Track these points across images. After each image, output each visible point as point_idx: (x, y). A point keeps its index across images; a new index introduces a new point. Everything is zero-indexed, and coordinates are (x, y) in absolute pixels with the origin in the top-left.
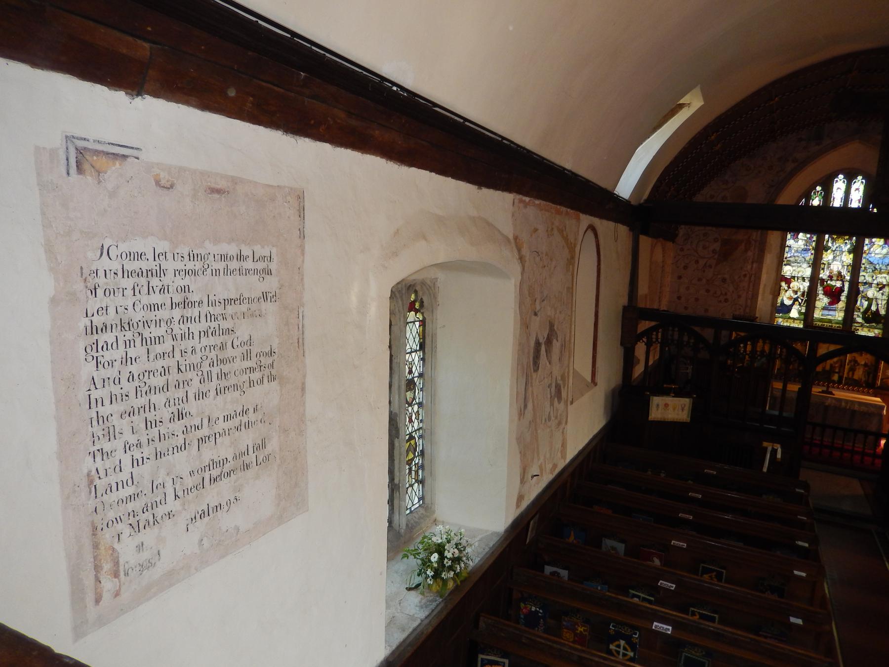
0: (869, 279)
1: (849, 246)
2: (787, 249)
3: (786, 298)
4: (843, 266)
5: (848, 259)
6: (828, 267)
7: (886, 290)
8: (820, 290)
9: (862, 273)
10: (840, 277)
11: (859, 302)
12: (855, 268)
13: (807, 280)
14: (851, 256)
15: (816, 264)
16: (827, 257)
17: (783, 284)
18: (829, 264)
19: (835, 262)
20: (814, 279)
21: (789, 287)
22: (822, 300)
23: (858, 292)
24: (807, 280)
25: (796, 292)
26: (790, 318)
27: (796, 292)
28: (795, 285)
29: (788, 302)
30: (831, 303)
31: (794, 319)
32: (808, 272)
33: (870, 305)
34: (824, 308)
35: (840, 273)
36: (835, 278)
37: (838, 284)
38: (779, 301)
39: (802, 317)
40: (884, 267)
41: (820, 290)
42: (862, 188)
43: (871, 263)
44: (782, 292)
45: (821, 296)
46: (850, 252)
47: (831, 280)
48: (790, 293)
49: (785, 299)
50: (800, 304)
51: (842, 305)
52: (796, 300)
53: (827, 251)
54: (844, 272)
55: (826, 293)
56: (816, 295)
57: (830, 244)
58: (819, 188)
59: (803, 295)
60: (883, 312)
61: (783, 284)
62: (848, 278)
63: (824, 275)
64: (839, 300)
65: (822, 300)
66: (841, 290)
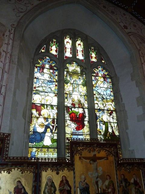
0: (102, 107)
1: (82, 81)
2: (35, 80)
3: (38, 125)
4: (81, 96)
5: (83, 90)
6: (70, 97)
7: (114, 114)
8: (67, 117)
9: (96, 102)
10: (81, 105)
11: (99, 126)
12: (90, 96)
13: (55, 108)
14: (85, 88)
15: (61, 94)
16: (68, 88)
17: (34, 111)
18: (70, 94)
19: (74, 93)
20: (61, 108)
21: (40, 114)
22: (70, 127)
23: (96, 117)
24: (55, 108)
25: (46, 119)
26: (44, 147)
27: (46, 119)
28: (44, 112)
29: (40, 130)
30: (78, 129)
31: (48, 147)
32: (54, 101)
33: (107, 128)
34: (73, 134)
35: (80, 101)
36: (77, 106)
37: (81, 111)
38: (31, 129)
39: (55, 144)
40: (108, 97)
41: (67, 117)
42: (82, 44)
43: (100, 94)
44: (34, 121)
45: (69, 122)
46: (84, 85)
47: (75, 107)
48: (41, 120)
49: (37, 126)
50: (51, 131)
51: (86, 130)
52: (47, 127)
53: (67, 83)
54: (83, 100)
55: (72, 120)
56: (65, 121)
57: (68, 79)
58: (54, 40)
59: (53, 122)
60: (117, 133)
61: (34, 111)
62: (86, 106)
63: (68, 103)
64: (83, 126)
65: (70, 127)
66: (83, 116)
